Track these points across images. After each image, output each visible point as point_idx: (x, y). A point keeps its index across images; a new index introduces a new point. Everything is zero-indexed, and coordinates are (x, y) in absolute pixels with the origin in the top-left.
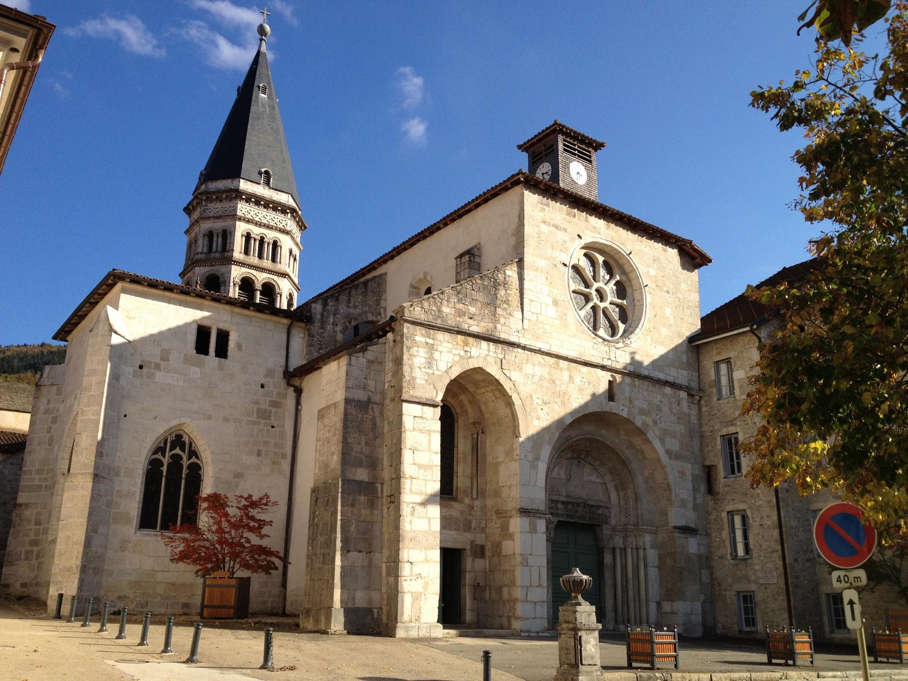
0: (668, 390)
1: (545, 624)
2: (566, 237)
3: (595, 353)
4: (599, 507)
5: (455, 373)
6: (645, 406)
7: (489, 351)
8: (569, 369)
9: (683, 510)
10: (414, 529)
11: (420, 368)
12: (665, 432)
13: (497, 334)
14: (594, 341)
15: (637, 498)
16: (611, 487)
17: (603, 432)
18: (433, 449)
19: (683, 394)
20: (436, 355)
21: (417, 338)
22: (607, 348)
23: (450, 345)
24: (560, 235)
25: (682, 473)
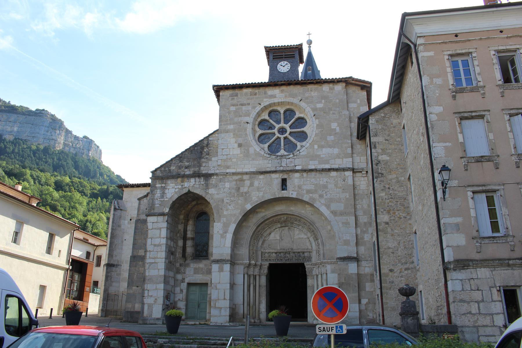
0: (334, 174)
1: (228, 318)
2: (249, 108)
3: (270, 165)
4: (303, 253)
5: (176, 197)
6: (312, 187)
7: (195, 182)
8: (250, 178)
9: (346, 247)
10: (150, 274)
11: (157, 199)
12: (331, 200)
13: (201, 172)
14: (269, 159)
15: (323, 244)
16: (312, 239)
17: (292, 208)
18: (162, 236)
19: (349, 174)
20: (166, 191)
21: (157, 186)
22: (279, 161)
23: (174, 185)
24: (244, 108)
25: (346, 224)
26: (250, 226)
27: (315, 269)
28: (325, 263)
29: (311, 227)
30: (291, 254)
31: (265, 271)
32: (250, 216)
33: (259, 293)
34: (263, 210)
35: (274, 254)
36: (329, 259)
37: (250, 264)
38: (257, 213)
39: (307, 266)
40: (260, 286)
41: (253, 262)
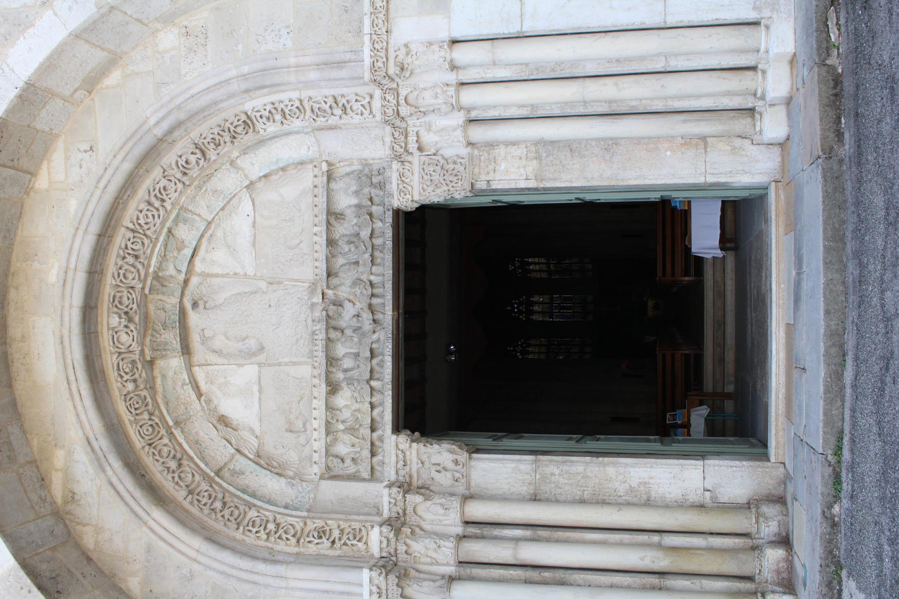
4: (333, 215)
16: (256, 164)
17: (53, 276)
26: (149, 549)
27: (428, 138)
28: (381, 49)
29: (169, 158)
30: (344, 292)
31: (439, 457)
32: (89, 541)
33: (582, 502)
34: (59, 458)
35: (342, 399)
36: (360, 31)
37: (390, 565)
38: (71, 497)
40: (535, 499)
41: (376, 540)
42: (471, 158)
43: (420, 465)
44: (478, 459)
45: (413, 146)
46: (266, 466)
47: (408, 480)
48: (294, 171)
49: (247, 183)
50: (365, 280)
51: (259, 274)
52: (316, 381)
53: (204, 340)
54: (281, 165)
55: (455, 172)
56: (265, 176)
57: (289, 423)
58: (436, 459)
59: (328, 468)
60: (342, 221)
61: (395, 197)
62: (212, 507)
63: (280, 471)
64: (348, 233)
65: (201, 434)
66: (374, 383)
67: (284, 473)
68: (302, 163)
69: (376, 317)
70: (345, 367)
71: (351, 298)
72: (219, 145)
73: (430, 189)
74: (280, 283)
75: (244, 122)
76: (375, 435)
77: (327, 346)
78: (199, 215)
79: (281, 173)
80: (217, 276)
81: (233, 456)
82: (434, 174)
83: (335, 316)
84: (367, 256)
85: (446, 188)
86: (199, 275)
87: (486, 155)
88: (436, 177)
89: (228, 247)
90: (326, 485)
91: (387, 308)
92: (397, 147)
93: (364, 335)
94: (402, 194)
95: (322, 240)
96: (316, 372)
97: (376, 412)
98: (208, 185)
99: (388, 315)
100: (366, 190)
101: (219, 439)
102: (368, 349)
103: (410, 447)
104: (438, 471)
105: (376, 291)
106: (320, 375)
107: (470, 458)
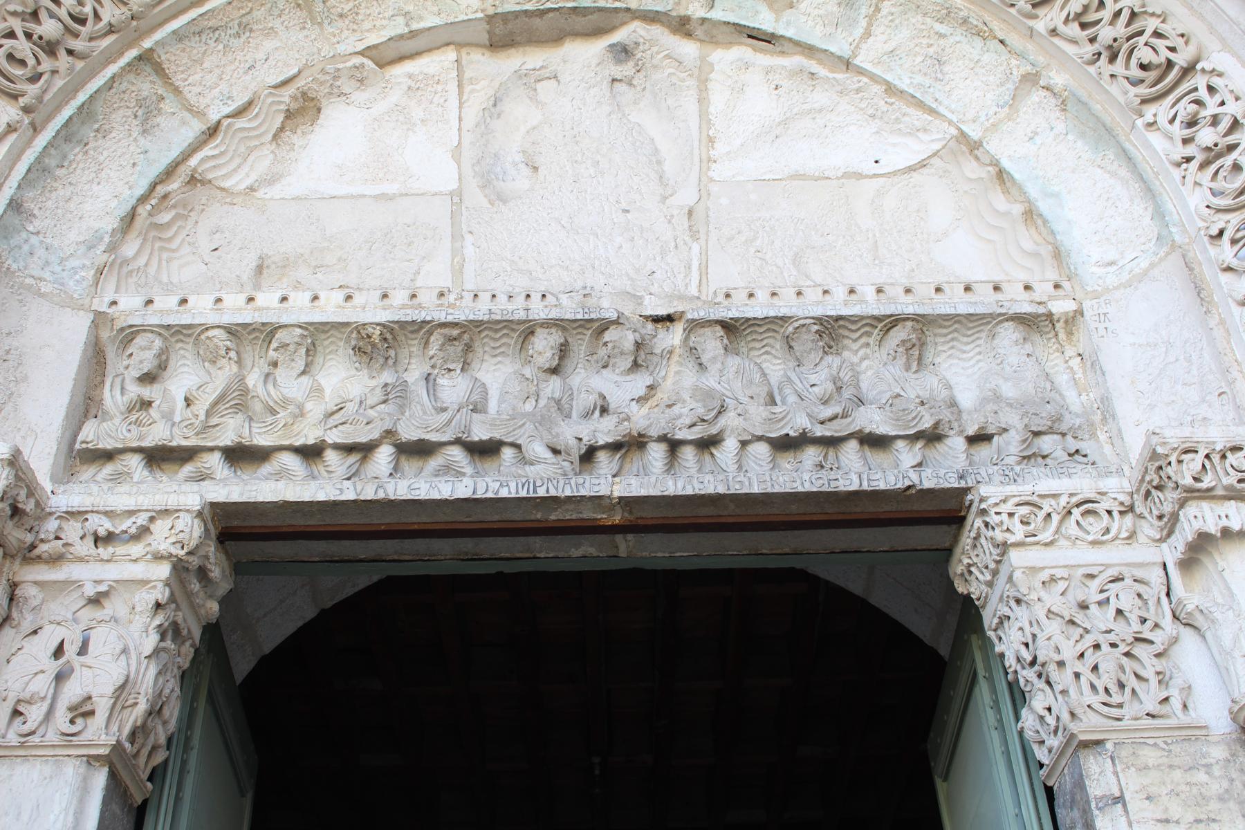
30: (678, 378)
35: (341, 378)
39: (1041, 581)
42: (1195, 733)
43: (90, 591)
44: (84, 789)
45: (1204, 517)
46: (161, 190)
47: (43, 548)
48: (1028, 245)
49: (974, 132)
50: (722, 422)
51: (714, 188)
52: (399, 297)
53: (530, 80)
54: (1043, 206)
55: (1132, 682)
56: (1002, 176)
57: (286, 265)
58: (104, 641)
59: (129, 335)
60: (901, 361)
61: (1011, 489)
62: (43, 15)
63: (139, 222)
64: (864, 386)
65: (269, 45)
66: (384, 454)
67: (133, 234)
68: (1058, 255)
69: (602, 456)
70: (440, 381)
71: (662, 396)
72: (1084, 26)
73: (1052, 599)
74: (694, 234)
75: (1170, 64)
76: (215, 459)
77: (506, 325)
78: (867, 34)
79: (1018, 209)
80: (703, 101)
81: (199, 114)
82: (1111, 612)
83: (602, 352)
84: (799, 422)
85: (1068, 654)
86: (703, 59)
87: (1216, 788)
88: (1101, 619)
89: (785, 123)
90: (76, 329)
91: (634, 481)
92: (1194, 463)
93: (542, 421)
94: (1024, 510)
95: (837, 306)
96: (427, 297)
97: (290, 461)
98: (959, 35)
99: (609, 482)
100: (1012, 418)
101: (253, 86)
102: (497, 435)
103: (158, 557)
104: (59, 652)
105: (688, 453)
106: (420, 307)
107: (92, 760)
